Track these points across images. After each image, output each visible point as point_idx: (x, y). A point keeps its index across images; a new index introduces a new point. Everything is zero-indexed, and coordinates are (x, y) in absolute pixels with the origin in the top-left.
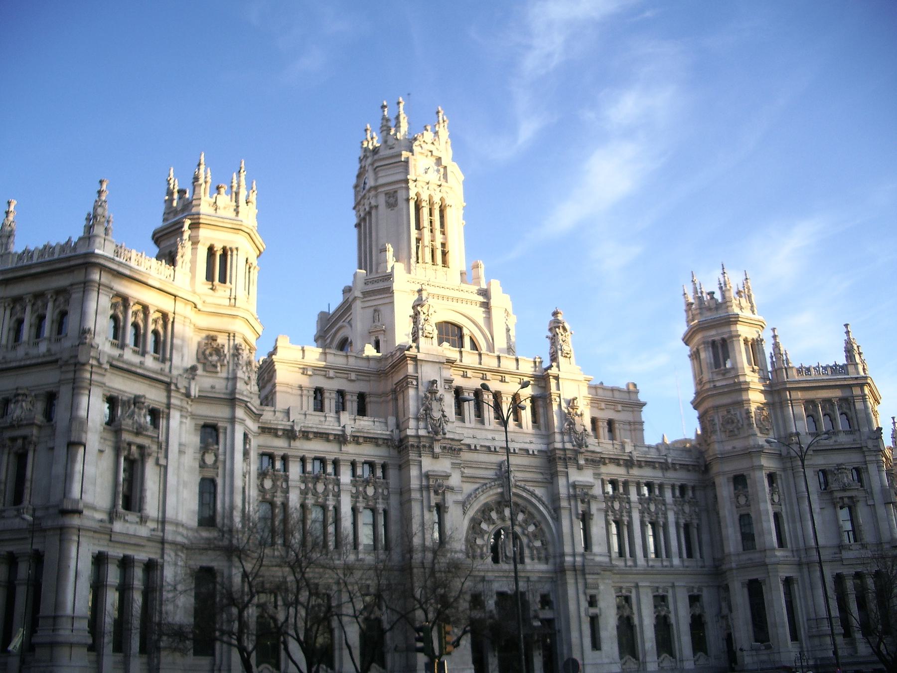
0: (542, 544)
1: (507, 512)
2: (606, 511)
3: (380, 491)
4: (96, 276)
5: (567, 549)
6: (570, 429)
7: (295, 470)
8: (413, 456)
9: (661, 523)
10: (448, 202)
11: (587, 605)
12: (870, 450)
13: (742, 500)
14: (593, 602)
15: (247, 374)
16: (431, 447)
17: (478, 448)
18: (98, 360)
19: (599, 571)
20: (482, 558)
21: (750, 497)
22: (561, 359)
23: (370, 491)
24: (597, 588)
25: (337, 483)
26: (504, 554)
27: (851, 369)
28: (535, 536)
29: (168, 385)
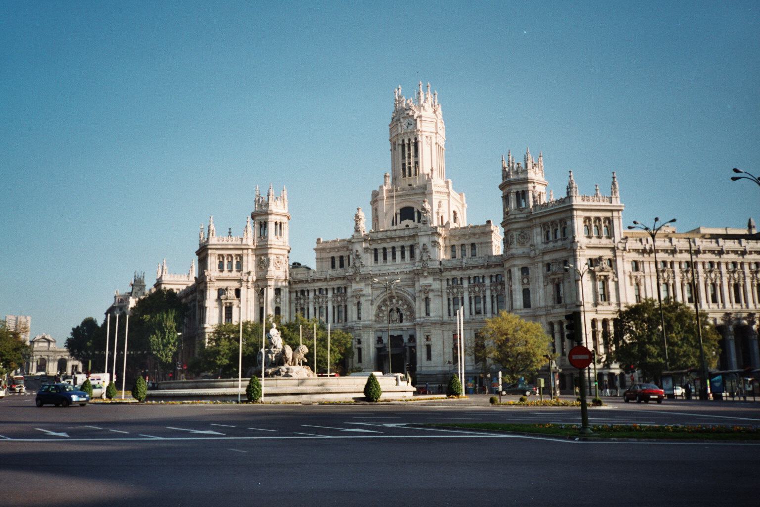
1: (394, 301)
2: (448, 294)
4: (210, 252)
6: (422, 259)
7: (312, 295)
9: (482, 297)
12: (570, 250)
13: (510, 282)
14: (428, 338)
16: (355, 279)
17: (381, 274)
23: (339, 299)
24: (430, 332)
25: (327, 297)
27: (567, 200)
29: (240, 281)
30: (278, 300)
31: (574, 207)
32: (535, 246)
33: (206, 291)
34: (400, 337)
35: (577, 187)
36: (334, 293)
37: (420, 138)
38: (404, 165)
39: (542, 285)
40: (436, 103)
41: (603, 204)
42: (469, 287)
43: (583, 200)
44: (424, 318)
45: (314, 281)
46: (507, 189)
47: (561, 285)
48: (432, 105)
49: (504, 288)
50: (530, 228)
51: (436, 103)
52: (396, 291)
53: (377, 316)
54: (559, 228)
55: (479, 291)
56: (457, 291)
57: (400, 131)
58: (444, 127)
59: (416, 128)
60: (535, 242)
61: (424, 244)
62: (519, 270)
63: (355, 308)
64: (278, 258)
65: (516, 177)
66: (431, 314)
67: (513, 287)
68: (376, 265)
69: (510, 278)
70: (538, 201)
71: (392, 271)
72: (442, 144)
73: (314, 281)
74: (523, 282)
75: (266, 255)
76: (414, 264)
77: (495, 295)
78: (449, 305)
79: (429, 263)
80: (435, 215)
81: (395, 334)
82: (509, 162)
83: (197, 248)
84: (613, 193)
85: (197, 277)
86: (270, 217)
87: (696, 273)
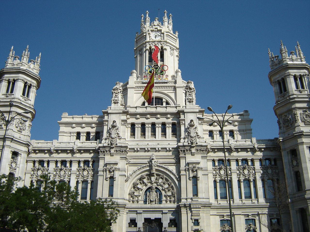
0: (172, 194)
1: (153, 179)
2: (215, 176)
5: (183, 196)
6: (188, 135)
7: (52, 166)
8: (101, 156)
13: (295, 163)
14: (197, 222)
17: (138, 149)
19: (200, 207)
20: (138, 202)
21: (298, 161)
22: (187, 103)
26: (149, 200)
28: (169, 190)
30: (14, 165)
34: (158, 221)
52: (157, 168)
53: (132, 195)
57: (148, 40)
59: (164, 39)
61: (192, 121)
62: (307, 147)
63: (107, 184)
71: (153, 147)
73: (57, 151)
76: (179, 141)
78: (215, 187)
79: (198, 140)
81: (153, 216)
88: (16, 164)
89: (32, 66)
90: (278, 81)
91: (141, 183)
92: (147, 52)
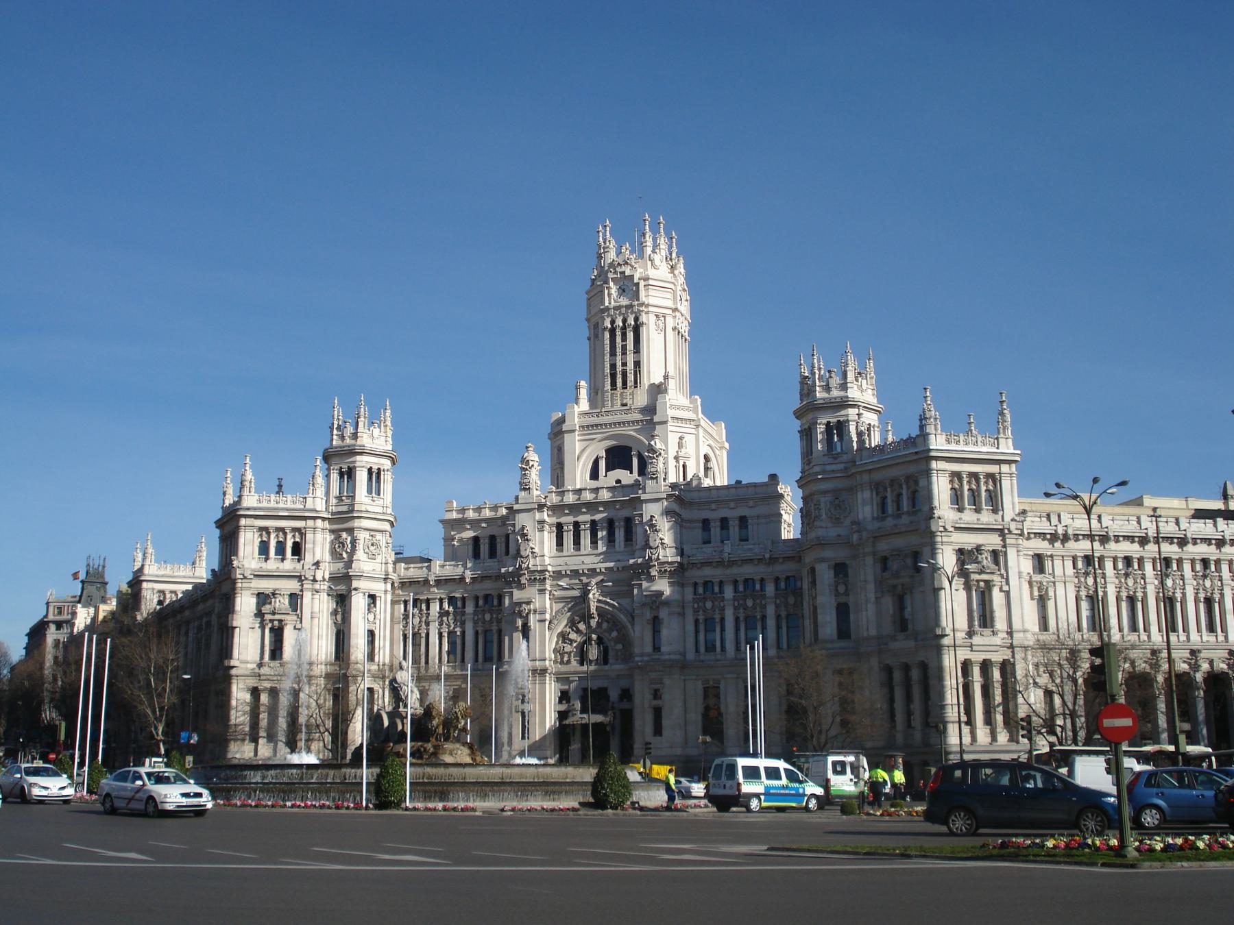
1: (593, 623)
2: (696, 611)
3: (495, 616)
4: (243, 522)
7: (435, 607)
9: (758, 617)
10: (640, 321)
11: (652, 697)
13: (813, 590)
14: (656, 695)
15: (370, 553)
18: (243, 575)
19: (661, 669)
20: (569, 662)
23: (487, 617)
24: (661, 683)
25: (463, 613)
31: (933, 454)
32: (859, 524)
33: (234, 598)
35: (938, 417)
36: (477, 605)
37: (643, 318)
38: (613, 366)
39: (872, 596)
40: (674, 255)
41: (985, 449)
42: (735, 599)
43: (948, 442)
44: (649, 655)
45: (439, 582)
46: (810, 416)
47: (908, 599)
48: (666, 258)
49: (802, 602)
50: (851, 490)
51: (674, 255)
54: (904, 492)
55: (754, 607)
56: (713, 606)
57: (607, 304)
58: (688, 298)
59: (638, 300)
60: (861, 516)
61: (651, 516)
64: (372, 536)
65: (825, 395)
66: (663, 649)
67: (820, 600)
68: (561, 554)
69: (814, 583)
70: (867, 442)
72: (685, 328)
74: (837, 590)
75: (350, 531)
77: (783, 614)
78: (697, 632)
80: (672, 463)
82: (813, 367)
83: (218, 514)
84: (1001, 431)
85: (217, 570)
86: (358, 458)
87: (1142, 578)
88: (375, 616)
89: (376, 431)
90: (805, 429)
91: (573, 630)
92: (607, 335)
